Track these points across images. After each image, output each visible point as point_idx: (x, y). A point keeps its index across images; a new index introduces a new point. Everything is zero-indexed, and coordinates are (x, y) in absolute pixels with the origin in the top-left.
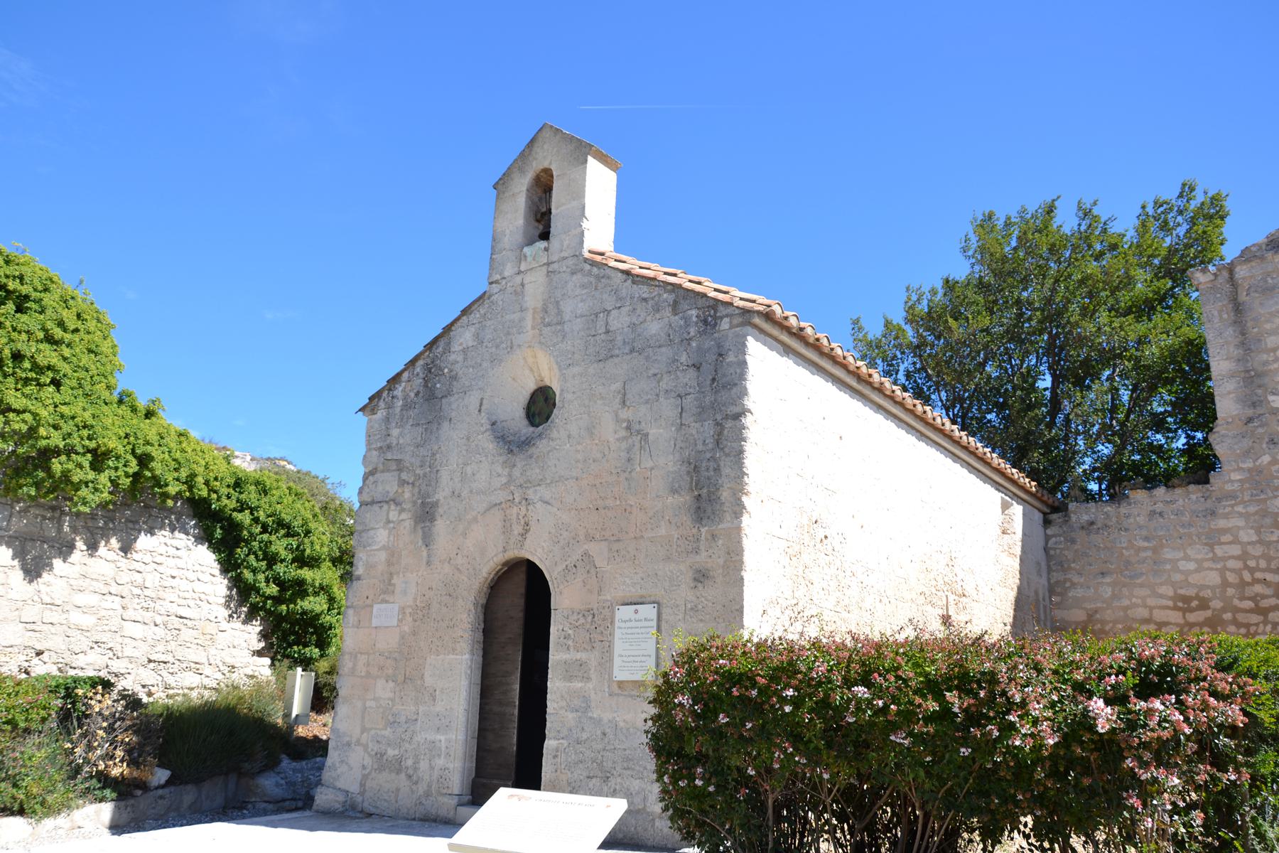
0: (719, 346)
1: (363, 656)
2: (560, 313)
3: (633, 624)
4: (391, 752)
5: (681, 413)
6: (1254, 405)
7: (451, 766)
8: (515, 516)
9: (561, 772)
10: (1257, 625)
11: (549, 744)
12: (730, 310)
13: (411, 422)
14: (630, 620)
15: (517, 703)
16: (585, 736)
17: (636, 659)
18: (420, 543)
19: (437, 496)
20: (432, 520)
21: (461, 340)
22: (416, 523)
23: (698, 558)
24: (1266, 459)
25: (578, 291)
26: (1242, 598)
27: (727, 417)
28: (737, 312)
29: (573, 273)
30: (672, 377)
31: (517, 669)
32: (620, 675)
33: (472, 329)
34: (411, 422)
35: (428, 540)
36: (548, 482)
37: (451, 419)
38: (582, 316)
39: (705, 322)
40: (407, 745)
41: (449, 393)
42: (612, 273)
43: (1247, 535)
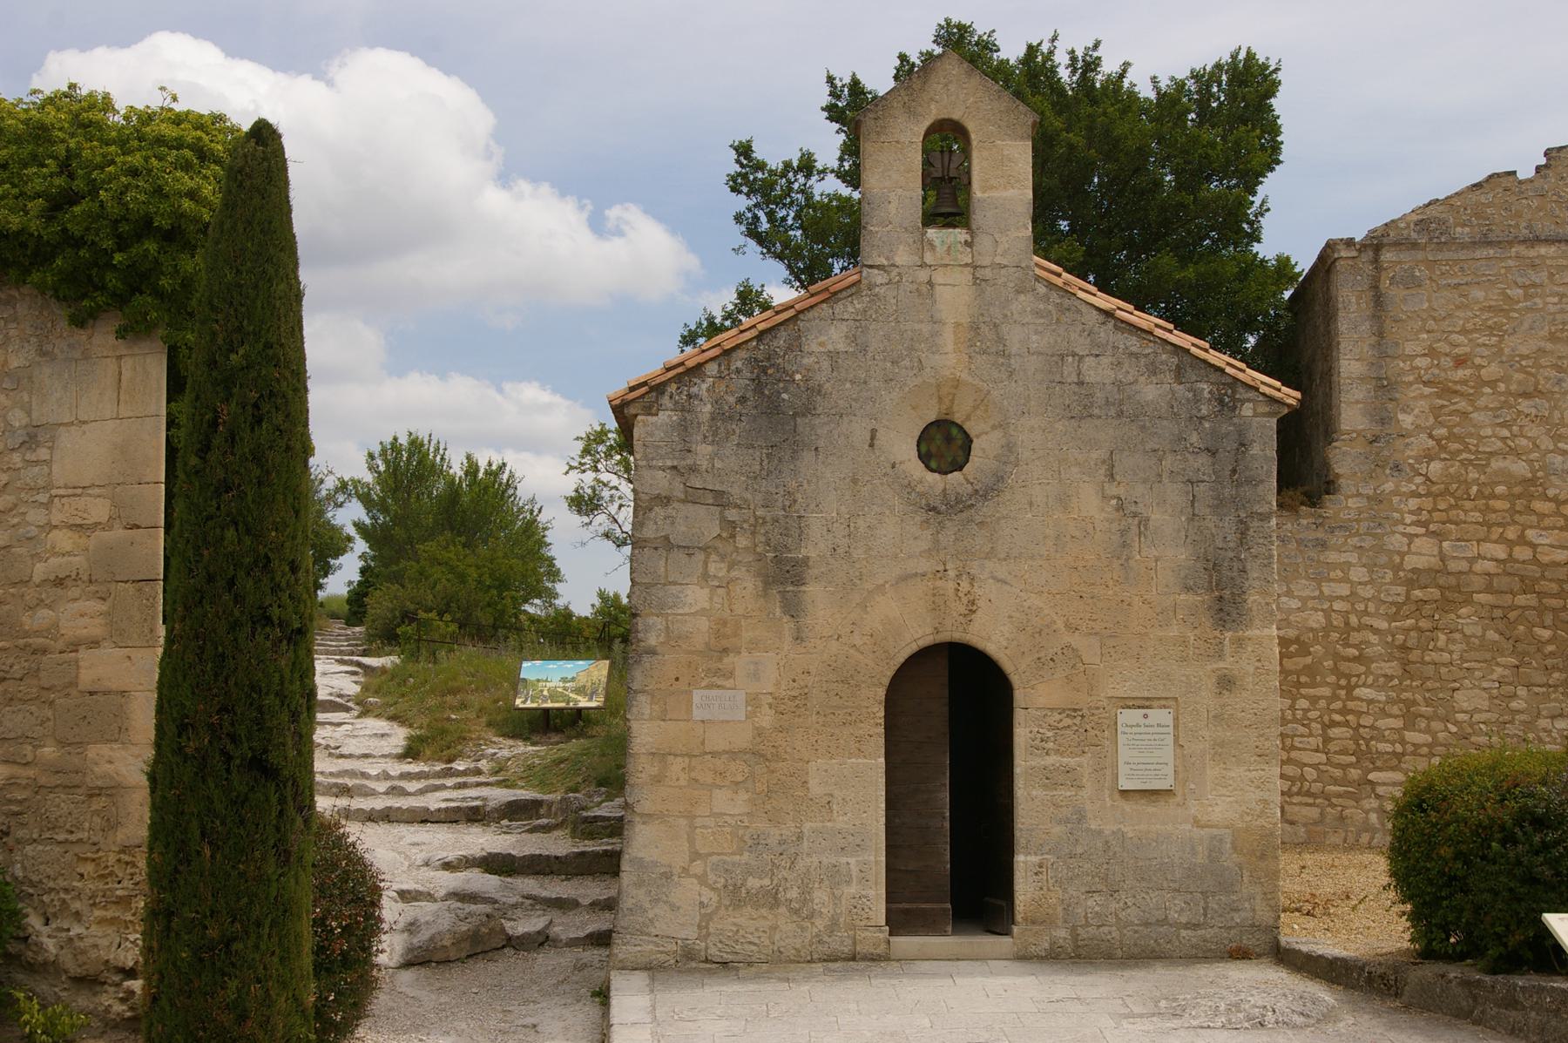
0: (1240, 433)
1: (679, 759)
2: (1000, 339)
3: (1142, 730)
4: (753, 883)
5: (1193, 502)
6: (1382, 422)
7: (872, 893)
8: (951, 592)
9: (1049, 890)
10: (1358, 676)
11: (1020, 859)
12: (1252, 394)
13: (735, 439)
14: (1138, 725)
15: (948, 814)
16: (1079, 850)
17: (1148, 767)
18: (778, 611)
19: (804, 552)
20: (799, 581)
21: (822, 339)
22: (767, 584)
23: (1221, 665)
24: (1389, 486)
25: (1028, 318)
26: (1346, 645)
27: (1252, 515)
28: (1261, 398)
29: (1018, 292)
30: (1179, 457)
31: (944, 774)
32: (1125, 784)
33: (844, 327)
34: (735, 439)
35: (793, 608)
36: (1002, 556)
37: (816, 449)
38: (1040, 353)
39: (1221, 402)
40: (785, 873)
41: (808, 410)
42: (1084, 308)
43: (1358, 574)
